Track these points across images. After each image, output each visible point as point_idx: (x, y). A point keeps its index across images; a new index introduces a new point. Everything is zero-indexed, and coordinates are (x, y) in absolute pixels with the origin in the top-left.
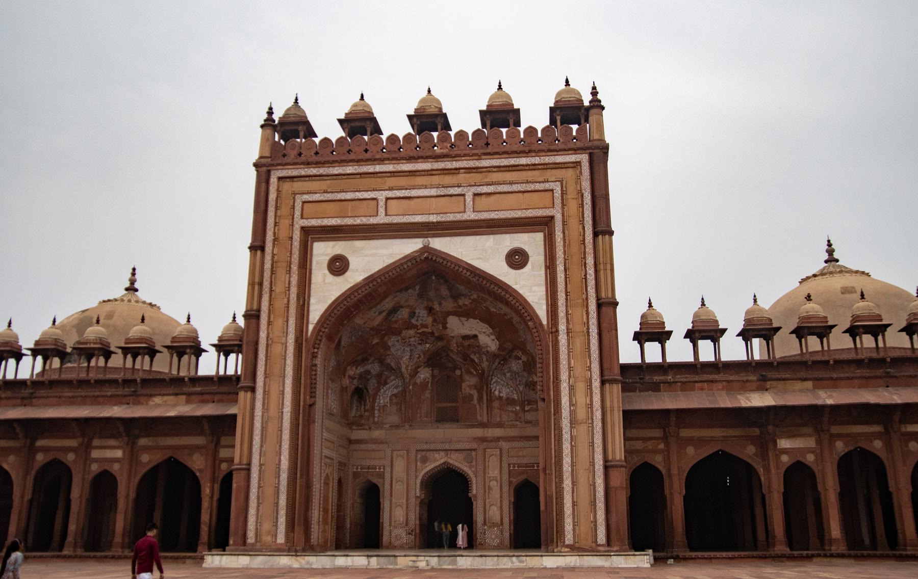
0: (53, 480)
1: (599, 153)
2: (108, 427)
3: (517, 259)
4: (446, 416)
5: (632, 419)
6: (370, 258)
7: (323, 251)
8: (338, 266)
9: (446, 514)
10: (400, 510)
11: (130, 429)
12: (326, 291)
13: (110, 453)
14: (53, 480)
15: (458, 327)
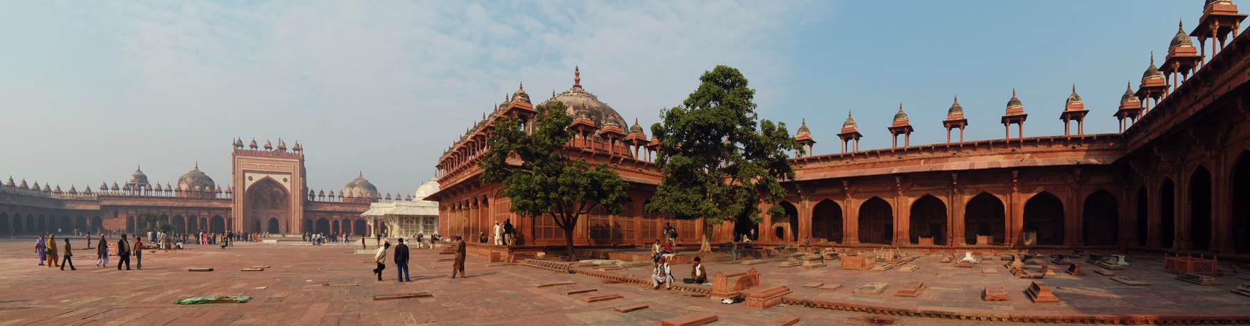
0: (192, 219)
1: (302, 161)
2: (203, 208)
3: (285, 180)
4: (274, 207)
5: (305, 212)
6: (257, 177)
7: (247, 175)
8: (251, 178)
9: (274, 228)
10: (264, 225)
11: (209, 209)
12: (248, 184)
13: (205, 213)
14: (192, 219)
15: (275, 189)
